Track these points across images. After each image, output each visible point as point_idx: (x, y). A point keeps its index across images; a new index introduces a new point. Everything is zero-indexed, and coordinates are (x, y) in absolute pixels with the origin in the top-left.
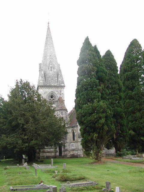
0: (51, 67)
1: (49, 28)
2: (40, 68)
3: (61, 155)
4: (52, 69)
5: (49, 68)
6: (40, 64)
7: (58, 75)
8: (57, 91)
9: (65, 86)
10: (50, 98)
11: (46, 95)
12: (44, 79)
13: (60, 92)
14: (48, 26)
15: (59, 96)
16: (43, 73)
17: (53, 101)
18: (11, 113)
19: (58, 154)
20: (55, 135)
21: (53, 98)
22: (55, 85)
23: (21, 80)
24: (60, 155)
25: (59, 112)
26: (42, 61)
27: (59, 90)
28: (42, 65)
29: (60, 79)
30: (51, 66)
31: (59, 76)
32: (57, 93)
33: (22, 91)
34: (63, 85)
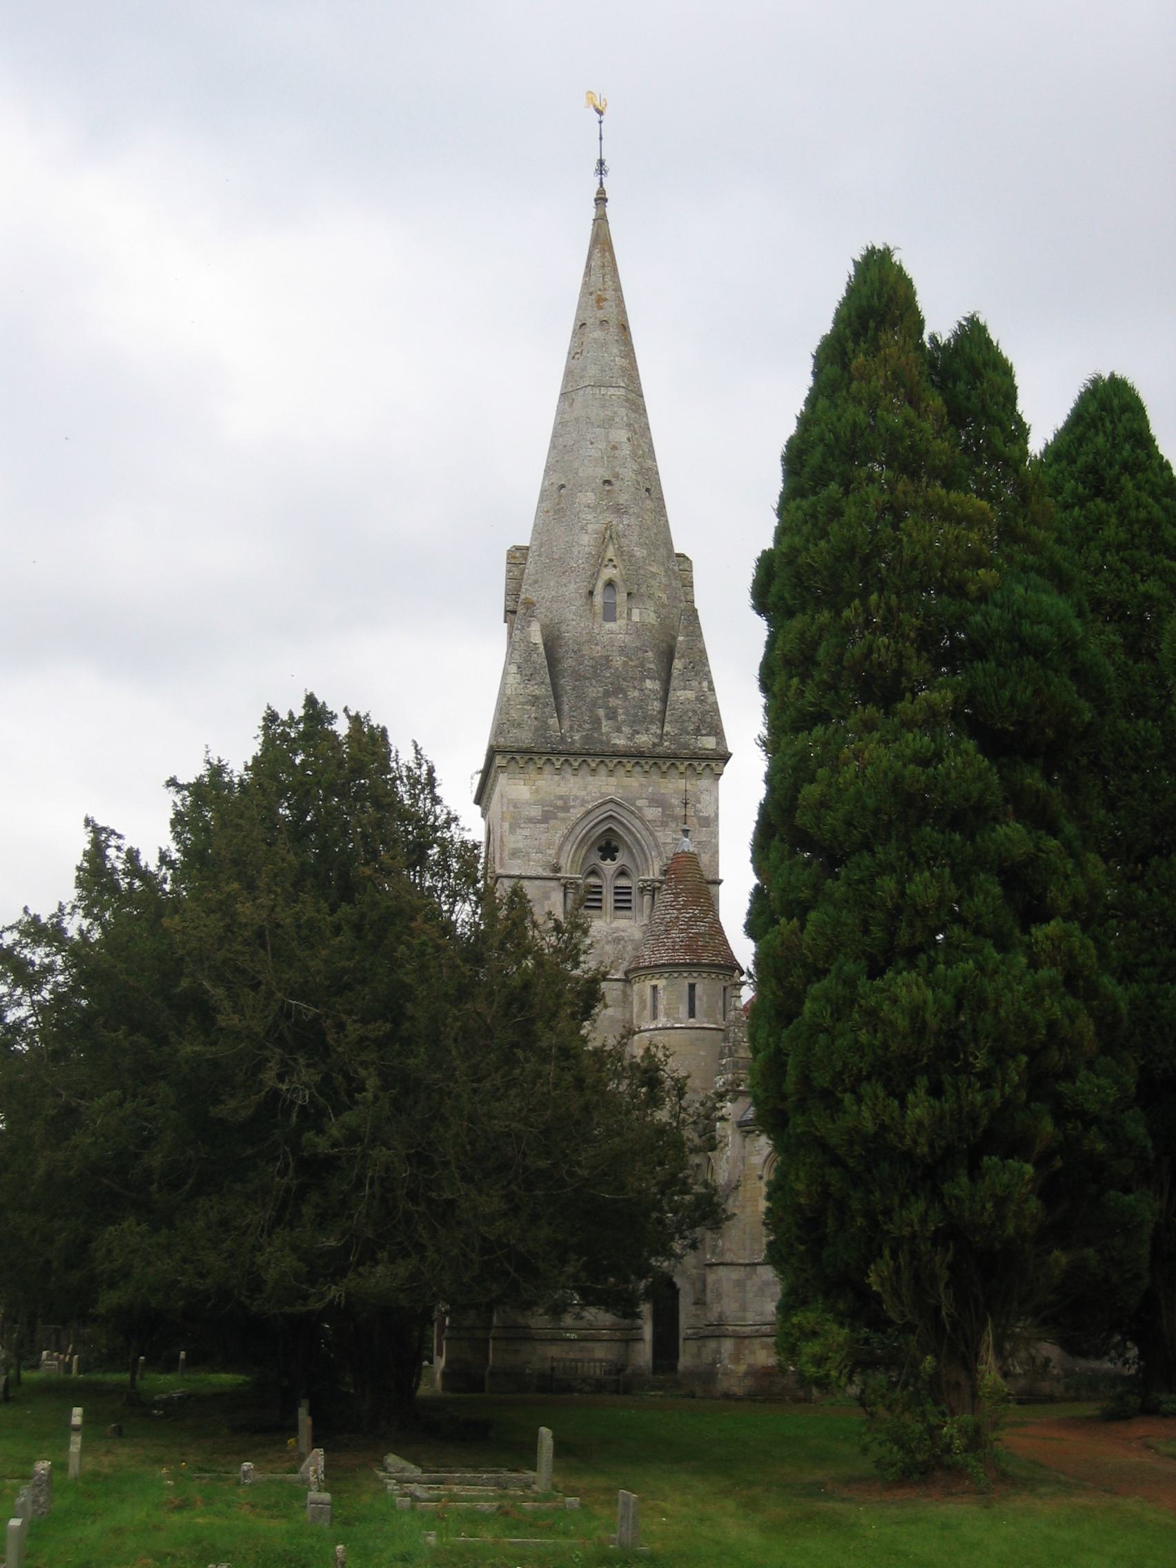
0: (610, 584)
1: (601, 241)
2: (514, 591)
3: (673, 1368)
4: (621, 597)
5: (591, 593)
6: (517, 557)
7: (668, 655)
8: (656, 801)
9: (725, 757)
10: (595, 858)
11: (562, 830)
12: (543, 691)
13: (679, 811)
14: (601, 221)
15: (670, 840)
16: (537, 638)
17: (623, 882)
18: (203, 1010)
19: (644, 1354)
20: (610, 1209)
21: (622, 859)
22: (644, 739)
23: (311, 701)
24: (656, 1368)
25: (661, 983)
26: (536, 531)
27: (673, 786)
28: (530, 568)
29: (682, 695)
30: (608, 573)
31: (678, 664)
32: (652, 813)
33: (313, 804)
34: (709, 743)
